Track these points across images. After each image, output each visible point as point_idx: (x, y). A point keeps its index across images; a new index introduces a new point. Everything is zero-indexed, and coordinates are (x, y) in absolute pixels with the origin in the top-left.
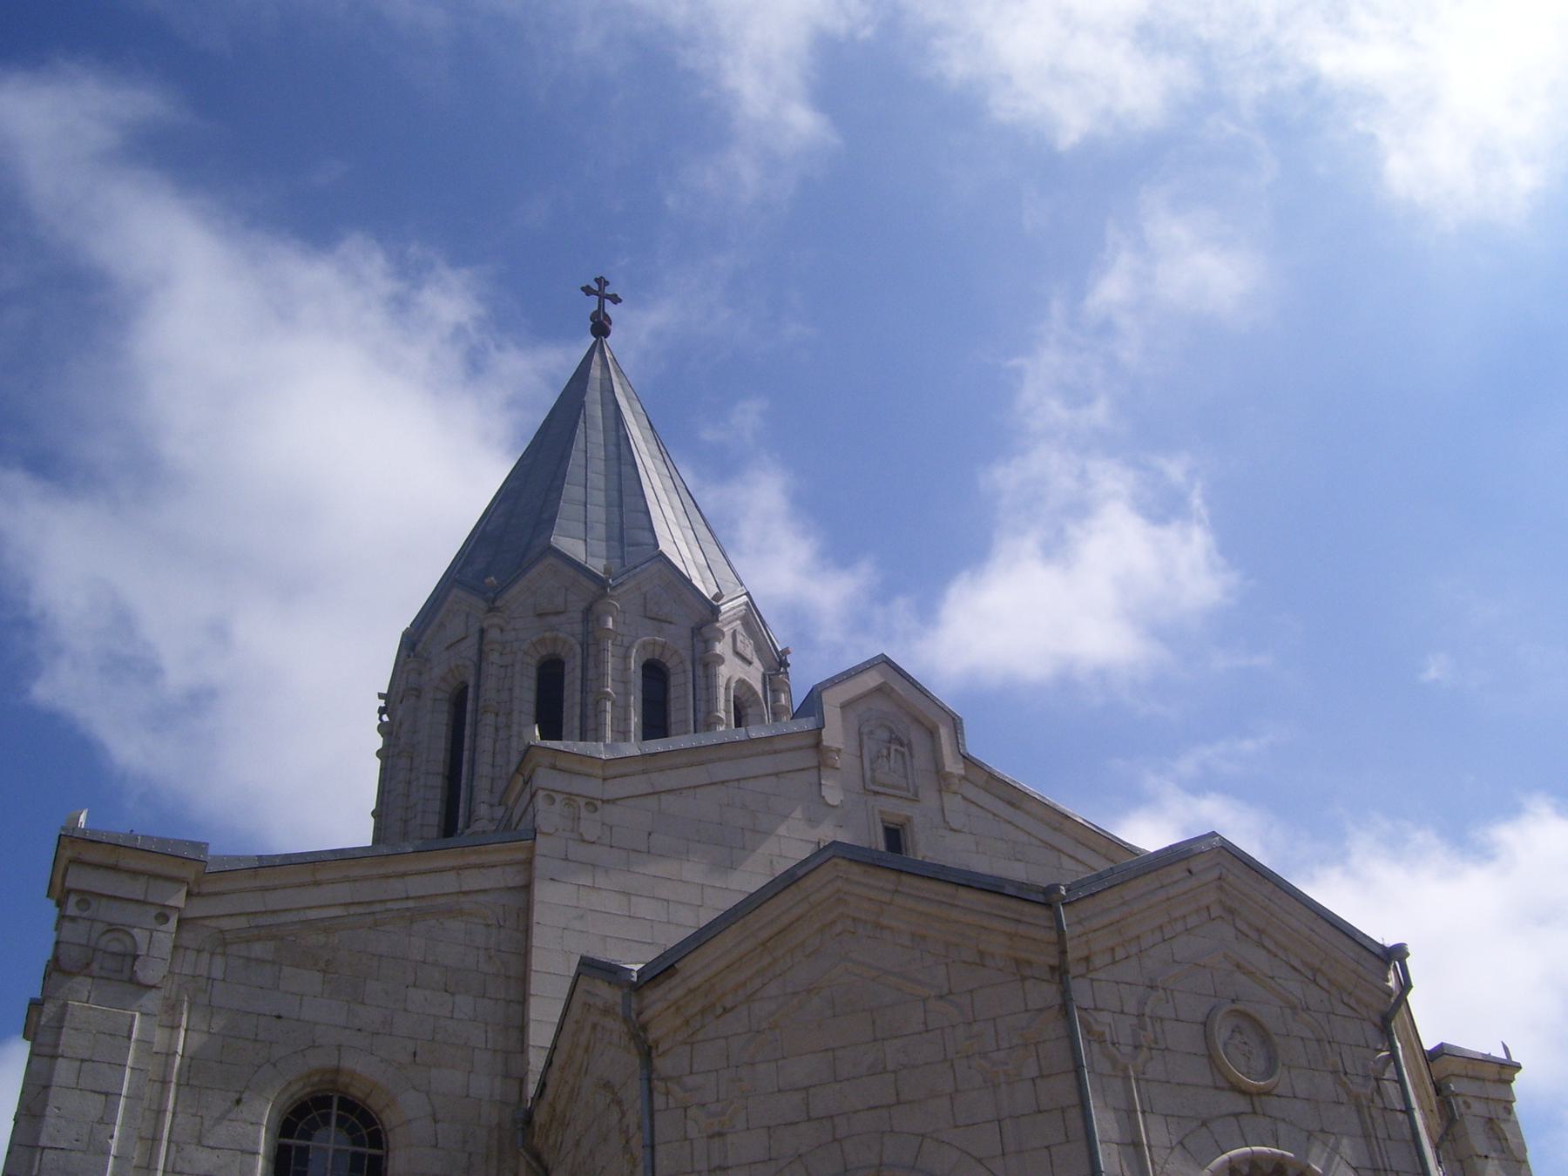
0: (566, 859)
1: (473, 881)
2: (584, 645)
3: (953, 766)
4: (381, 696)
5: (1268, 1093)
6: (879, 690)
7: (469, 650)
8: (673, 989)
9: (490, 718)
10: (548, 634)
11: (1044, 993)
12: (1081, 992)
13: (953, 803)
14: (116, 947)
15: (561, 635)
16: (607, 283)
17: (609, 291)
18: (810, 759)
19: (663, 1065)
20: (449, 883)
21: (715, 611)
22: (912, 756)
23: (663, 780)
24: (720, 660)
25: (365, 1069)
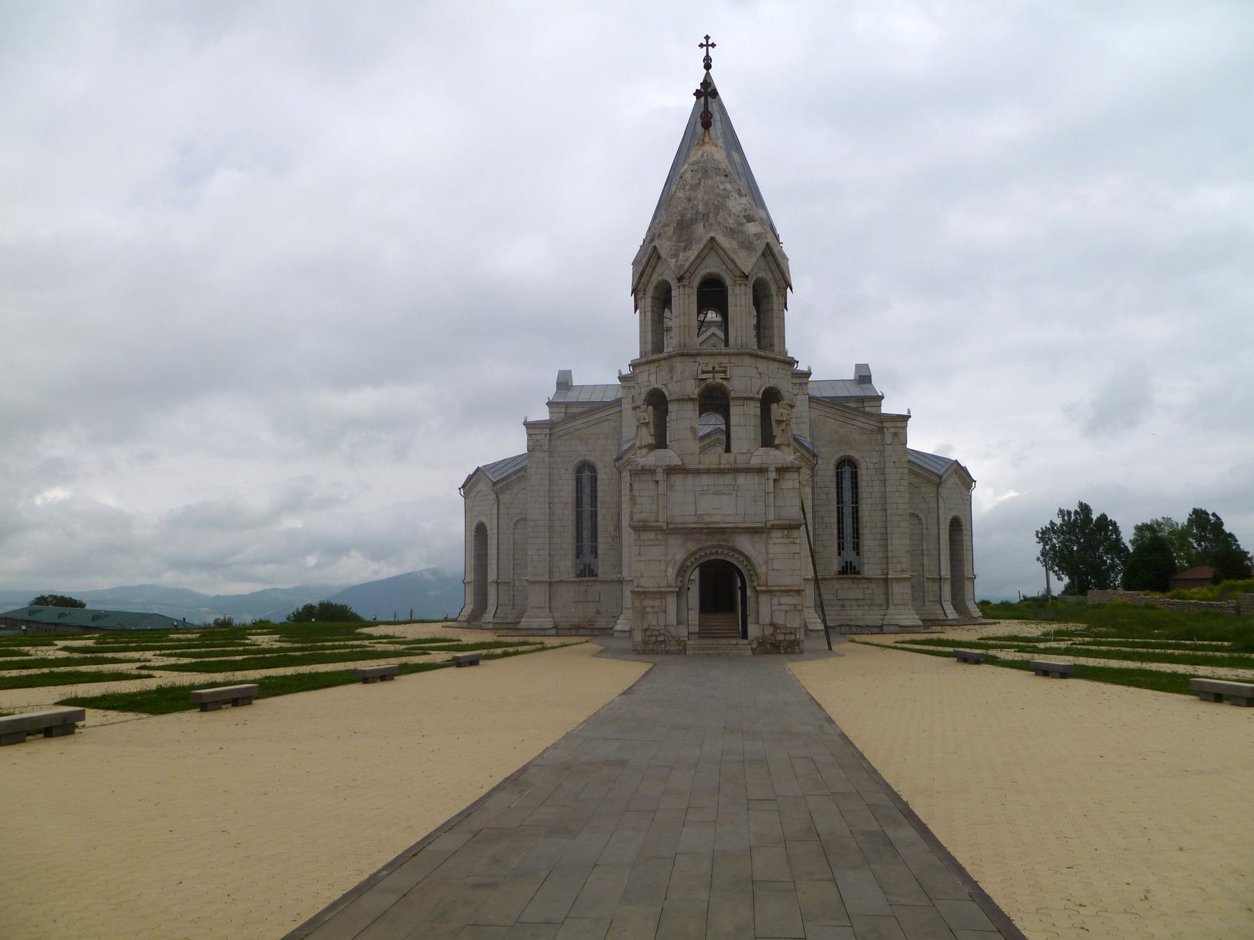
8: (622, 461)
20: (603, 414)
25: (591, 459)
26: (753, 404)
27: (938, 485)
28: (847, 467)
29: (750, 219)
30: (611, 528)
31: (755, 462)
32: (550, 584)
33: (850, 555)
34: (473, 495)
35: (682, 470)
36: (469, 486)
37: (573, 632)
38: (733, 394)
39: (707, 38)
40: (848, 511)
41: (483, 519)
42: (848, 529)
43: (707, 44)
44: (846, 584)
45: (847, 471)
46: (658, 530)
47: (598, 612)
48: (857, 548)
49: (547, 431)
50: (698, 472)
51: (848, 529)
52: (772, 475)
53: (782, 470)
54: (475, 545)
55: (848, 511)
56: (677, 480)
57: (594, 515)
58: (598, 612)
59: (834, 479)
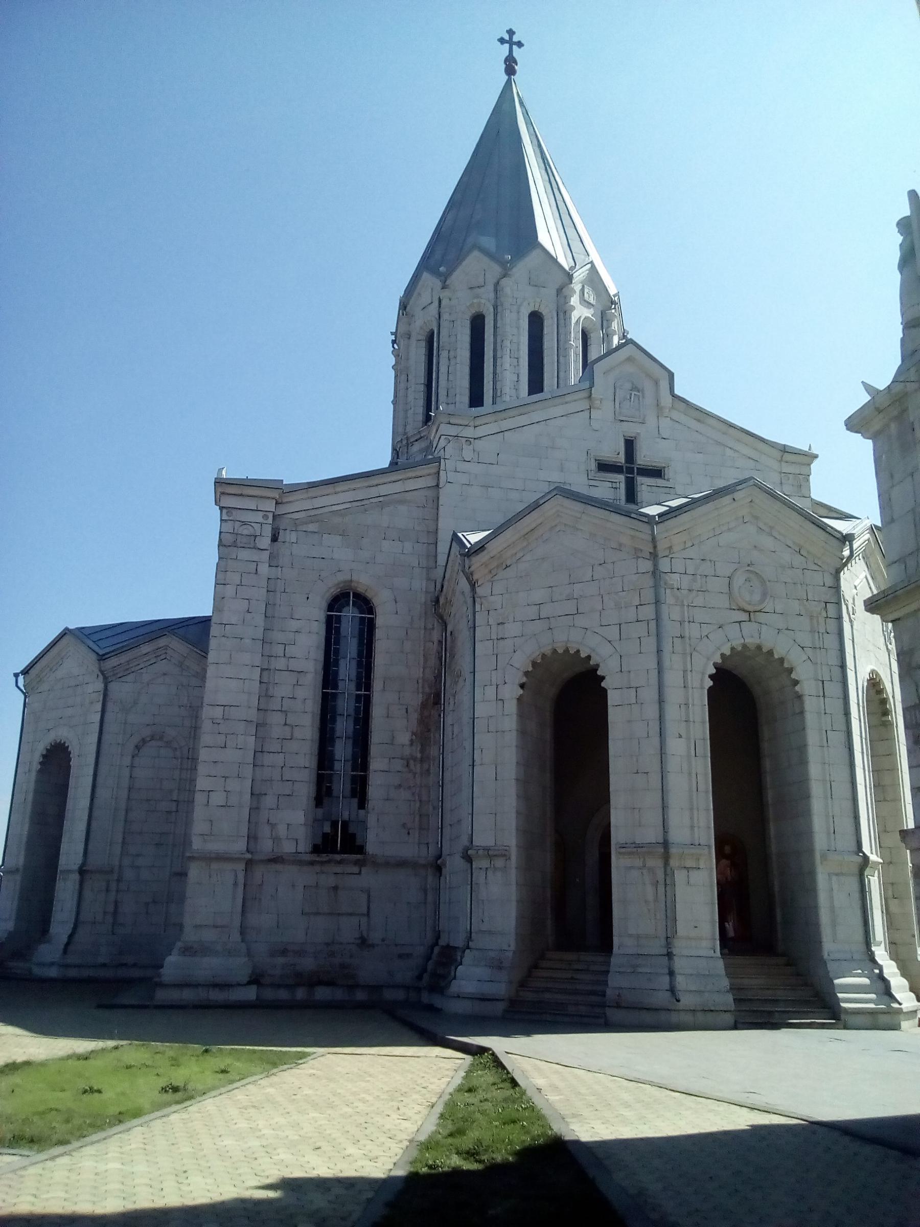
0: (456, 471)
1: (411, 485)
2: (495, 307)
3: (666, 400)
4: (392, 333)
5: (760, 611)
6: (630, 359)
7: (434, 308)
8: (483, 557)
9: (444, 354)
10: (475, 301)
11: (646, 565)
12: (664, 565)
13: (665, 423)
14: (245, 532)
15: (483, 301)
16: (514, 33)
17: (515, 39)
18: (585, 405)
19: (479, 590)
20: (398, 487)
21: (570, 277)
22: (643, 397)
23: (505, 425)
24: (573, 308)
25: (364, 581)
30: (404, 738)
32: (249, 864)
34: (44, 687)
36: (32, 675)
37: (301, 994)
39: (511, 32)
41: (63, 734)
43: (510, 40)
47: (363, 942)
49: (270, 506)
54: (36, 792)
57: (364, 704)
58: (363, 942)
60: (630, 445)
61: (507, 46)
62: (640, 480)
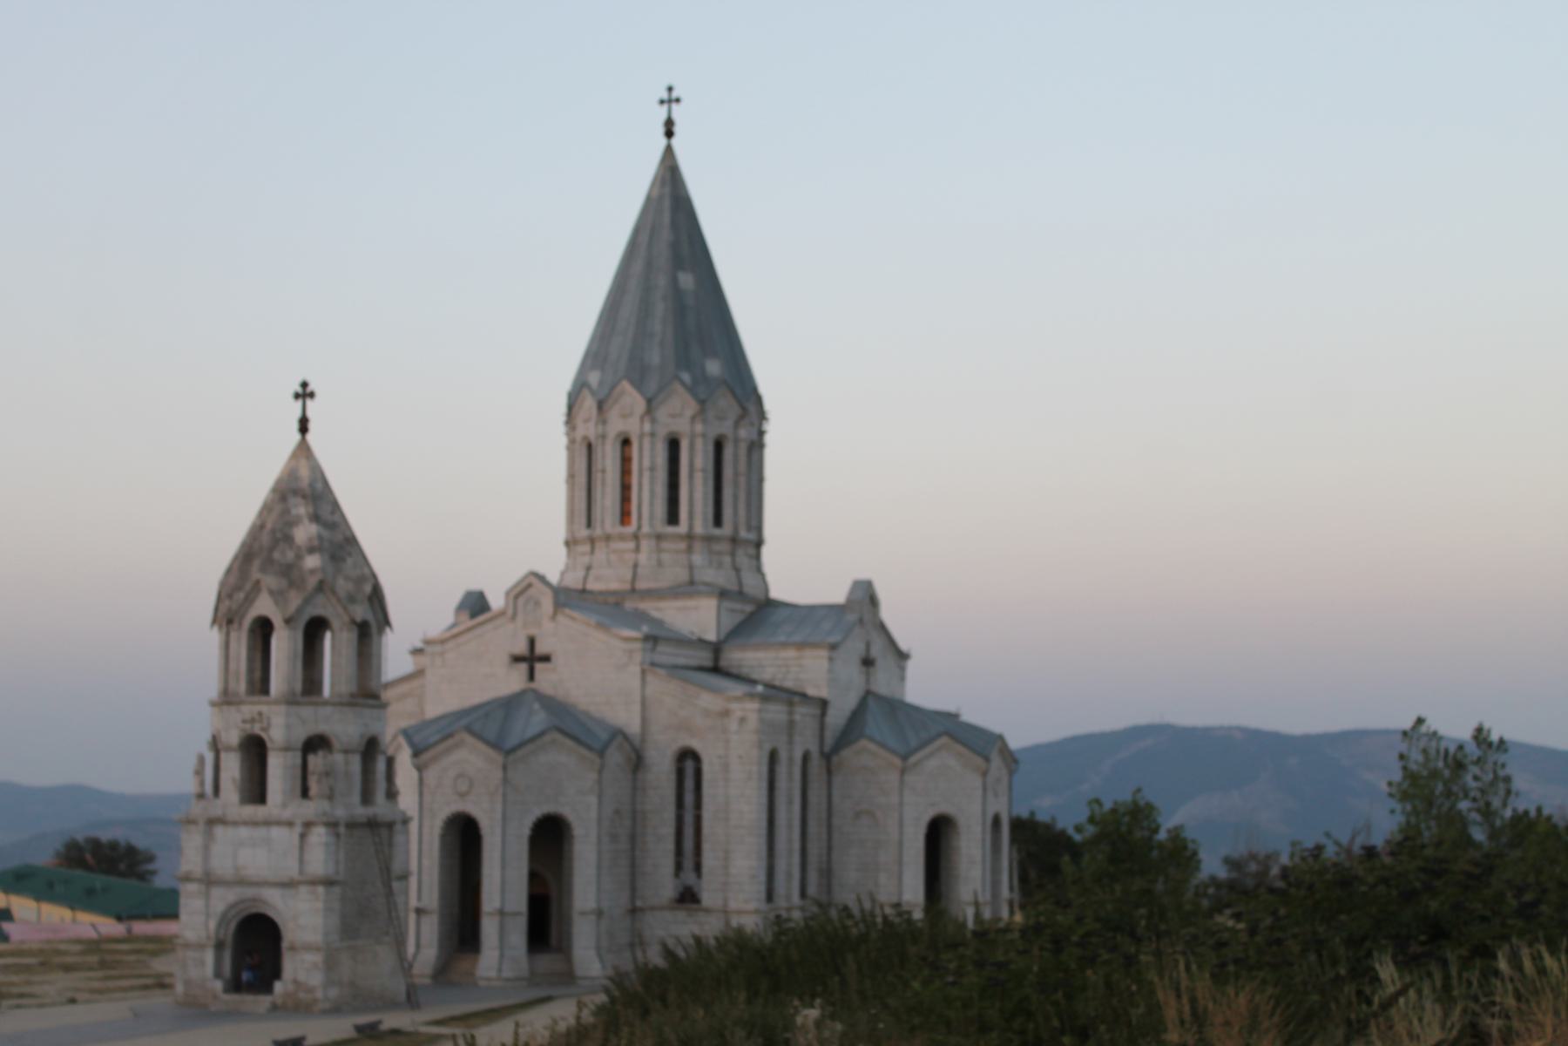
26: (290, 754)
27: (903, 772)
28: (688, 758)
29: (311, 550)
31: (287, 814)
33: (689, 877)
35: (221, 821)
38: (269, 745)
39: (670, 89)
40: (689, 819)
42: (688, 844)
43: (670, 100)
44: (681, 915)
45: (689, 765)
46: (199, 881)
48: (698, 868)
50: (235, 824)
51: (688, 844)
52: (298, 829)
53: (308, 825)
55: (689, 819)
56: (219, 831)
59: (673, 777)
60: (532, 642)
61: (665, 107)
62: (539, 666)
